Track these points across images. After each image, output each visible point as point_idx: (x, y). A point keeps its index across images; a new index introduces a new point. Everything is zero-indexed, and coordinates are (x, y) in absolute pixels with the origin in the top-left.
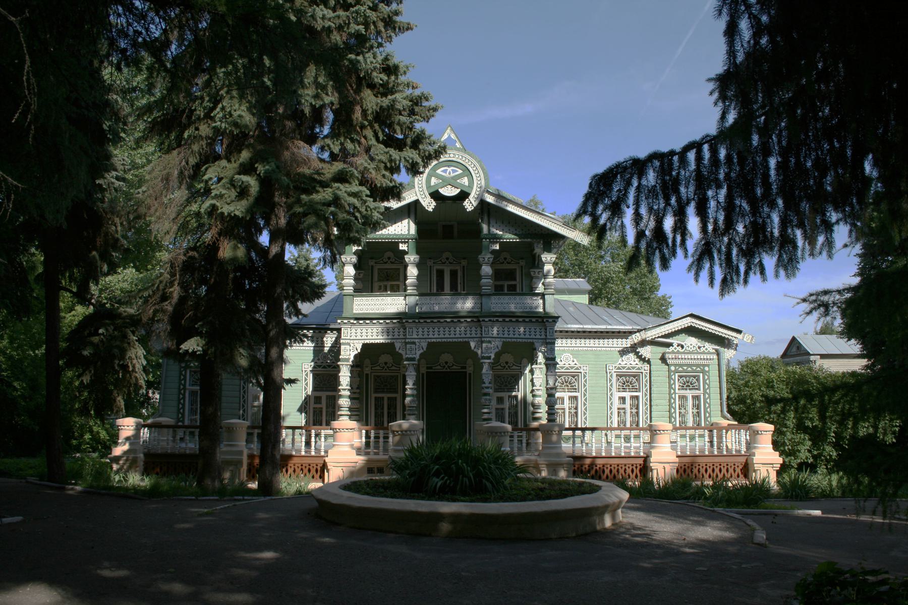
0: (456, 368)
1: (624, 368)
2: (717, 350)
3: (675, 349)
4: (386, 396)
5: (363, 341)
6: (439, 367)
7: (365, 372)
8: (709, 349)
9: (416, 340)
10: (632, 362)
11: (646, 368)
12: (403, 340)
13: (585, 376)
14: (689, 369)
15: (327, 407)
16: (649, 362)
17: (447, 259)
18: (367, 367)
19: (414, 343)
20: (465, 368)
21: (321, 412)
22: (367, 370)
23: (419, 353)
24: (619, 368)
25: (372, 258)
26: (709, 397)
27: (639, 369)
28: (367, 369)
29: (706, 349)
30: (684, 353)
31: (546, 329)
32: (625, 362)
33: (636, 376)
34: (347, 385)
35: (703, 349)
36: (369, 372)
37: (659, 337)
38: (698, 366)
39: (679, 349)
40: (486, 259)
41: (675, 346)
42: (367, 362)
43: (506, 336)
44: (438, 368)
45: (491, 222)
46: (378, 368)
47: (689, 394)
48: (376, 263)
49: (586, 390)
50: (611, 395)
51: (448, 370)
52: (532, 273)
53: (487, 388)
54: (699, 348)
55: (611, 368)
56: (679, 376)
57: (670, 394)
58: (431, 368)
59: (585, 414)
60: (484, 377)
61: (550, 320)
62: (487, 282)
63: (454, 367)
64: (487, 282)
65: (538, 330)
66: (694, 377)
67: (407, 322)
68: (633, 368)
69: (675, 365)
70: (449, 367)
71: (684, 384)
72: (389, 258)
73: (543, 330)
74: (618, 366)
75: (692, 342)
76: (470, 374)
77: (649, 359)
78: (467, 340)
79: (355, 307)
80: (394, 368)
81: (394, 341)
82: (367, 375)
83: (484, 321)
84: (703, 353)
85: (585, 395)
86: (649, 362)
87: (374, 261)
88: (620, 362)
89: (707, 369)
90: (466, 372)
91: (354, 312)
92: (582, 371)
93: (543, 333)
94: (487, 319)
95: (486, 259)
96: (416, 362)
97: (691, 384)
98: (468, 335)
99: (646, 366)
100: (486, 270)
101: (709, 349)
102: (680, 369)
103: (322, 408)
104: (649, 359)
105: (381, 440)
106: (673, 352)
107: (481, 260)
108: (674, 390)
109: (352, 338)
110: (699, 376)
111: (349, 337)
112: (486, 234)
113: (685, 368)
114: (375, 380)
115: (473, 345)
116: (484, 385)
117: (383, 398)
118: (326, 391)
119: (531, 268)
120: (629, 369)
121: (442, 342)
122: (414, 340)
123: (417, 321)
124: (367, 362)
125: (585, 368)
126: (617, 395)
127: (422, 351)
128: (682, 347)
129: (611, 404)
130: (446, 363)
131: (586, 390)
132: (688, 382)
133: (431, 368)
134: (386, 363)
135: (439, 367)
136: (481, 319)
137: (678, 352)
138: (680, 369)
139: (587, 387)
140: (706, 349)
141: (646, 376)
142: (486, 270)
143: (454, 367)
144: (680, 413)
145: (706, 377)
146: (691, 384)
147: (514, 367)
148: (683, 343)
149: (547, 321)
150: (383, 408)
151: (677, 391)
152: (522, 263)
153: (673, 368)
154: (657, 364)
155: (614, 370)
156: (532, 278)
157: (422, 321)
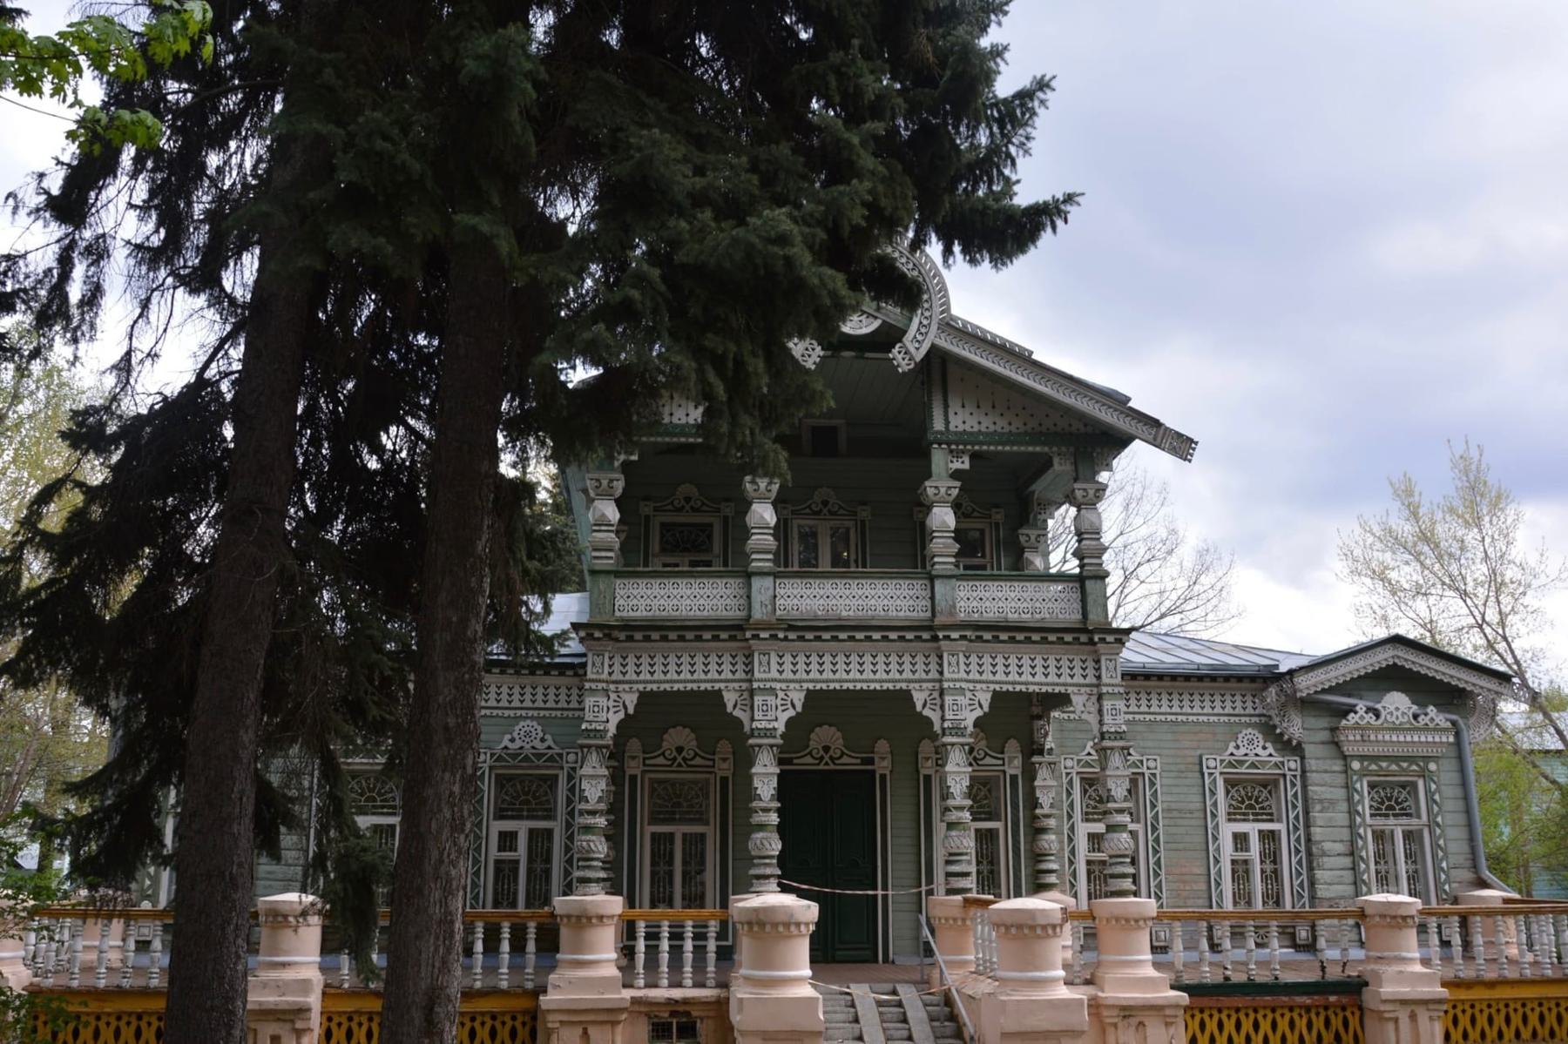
0: (850, 762)
1: (1241, 763)
2: (1454, 723)
3: (1362, 718)
4: (679, 830)
5: (641, 687)
6: (808, 760)
7: (629, 772)
8: (1437, 721)
9: (778, 686)
10: (1259, 751)
11: (1293, 765)
12: (744, 685)
13: (1152, 784)
14: (1394, 767)
15: (530, 860)
16: (1296, 749)
17: (825, 503)
18: (634, 758)
19: (772, 691)
20: (871, 761)
21: (515, 871)
22: (633, 768)
23: (784, 717)
24: (1230, 765)
25: (646, 498)
26: (1443, 835)
28: (633, 763)
29: (1432, 720)
30: (1378, 729)
31: (1098, 661)
32: (1243, 751)
33: (1270, 784)
34: (600, 799)
35: (1423, 720)
36: (638, 772)
37: (1324, 691)
38: (1411, 759)
39: (1370, 718)
40: (943, 490)
41: (1361, 712)
42: (634, 745)
43: (1000, 677)
44: (805, 762)
45: (950, 403)
46: (661, 760)
47: (1397, 827)
48: (656, 509)
49: (1156, 817)
50: (1216, 827)
51: (832, 767)
52: (1022, 539)
53: (961, 808)
54: (1415, 717)
55: (1212, 763)
57: (1352, 826)
58: (789, 761)
59: (1157, 875)
60: (950, 782)
61: (1110, 638)
62: (943, 549)
63: (845, 760)
64: (943, 549)
65: (1077, 664)
66: (1403, 786)
67: (756, 637)
68: (1264, 763)
69: (1362, 758)
70: (831, 758)
71: (1382, 803)
72: (688, 500)
73: (1090, 664)
74: (1228, 758)
75: (1397, 703)
76: (883, 777)
77: (1299, 744)
78: (904, 686)
79: (619, 602)
80: (698, 761)
81: (722, 686)
82: (633, 778)
83: (947, 638)
84: (1426, 729)
85: (1154, 829)
86: (1296, 749)
87: (652, 505)
88: (1231, 749)
89: (1432, 766)
90: (873, 772)
91: (617, 614)
92: (1144, 770)
93: (1090, 672)
94: (955, 635)
95: (943, 490)
96: (780, 741)
98: (907, 675)
99: (1293, 764)
100: (943, 518)
101: (1437, 721)
102: (1373, 767)
103: (517, 862)
104: (1299, 744)
105: (665, 945)
106: (1357, 727)
107: (930, 491)
108: (1363, 816)
109: (614, 677)
110: (1414, 785)
111: (605, 676)
112: (941, 433)
113: (1384, 765)
114: (653, 791)
115: (919, 698)
116: (950, 802)
117: (672, 835)
118: (528, 818)
119: (1021, 526)
120: (1253, 765)
121: (841, 691)
122: (774, 685)
123: (781, 635)
124: (634, 745)
125: (1152, 764)
126: (1227, 830)
127: (791, 713)
128: (1378, 716)
129: (1218, 849)
130: (826, 749)
131: (1156, 817)
132: (1389, 799)
133: (789, 761)
134: (680, 750)
135: (808, 760)
136: (941, 635)
137: (1369, 727)
138: (1373, 767)
139: (1159, 808)
141: (1293, 785)
142: (943, 518)
143: (845, 760)
144: (1377, 872)
145: (1433, 787)
146: (1398, 803)
147: (988, 760)
148: (1378, 706)
149: (1103, 640)
150: (671, 862)
151: (1368, 820)
152: (998, 516)
153: (1356, 765)
154: (1318, 758)
155: (1220, 769)
156: (1021, 551)
157: (792, 636)
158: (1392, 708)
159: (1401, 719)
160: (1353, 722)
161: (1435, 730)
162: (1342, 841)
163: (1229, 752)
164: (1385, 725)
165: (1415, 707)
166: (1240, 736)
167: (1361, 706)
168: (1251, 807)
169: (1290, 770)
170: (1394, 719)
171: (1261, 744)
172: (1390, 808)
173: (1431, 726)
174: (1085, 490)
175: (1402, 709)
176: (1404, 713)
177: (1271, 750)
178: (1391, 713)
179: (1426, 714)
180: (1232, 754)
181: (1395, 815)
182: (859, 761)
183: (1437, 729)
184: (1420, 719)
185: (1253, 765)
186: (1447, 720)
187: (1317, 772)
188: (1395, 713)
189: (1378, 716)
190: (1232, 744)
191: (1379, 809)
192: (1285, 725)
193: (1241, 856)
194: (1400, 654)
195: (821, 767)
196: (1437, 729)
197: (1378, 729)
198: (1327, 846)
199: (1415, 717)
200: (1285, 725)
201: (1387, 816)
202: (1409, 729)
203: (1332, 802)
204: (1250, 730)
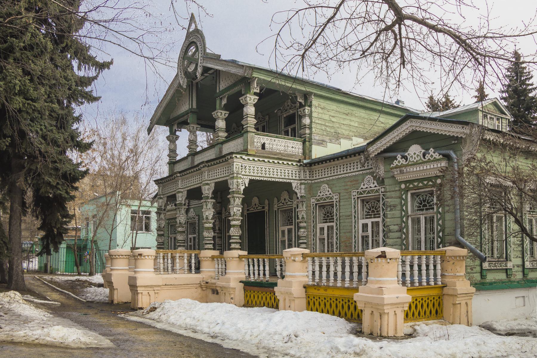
1: (364, 192)
14: (421, 185)
27: (377, 191)
30: (406, 166)
35: (428, 157)
39: (403, 162)
51: (257, 211)
54: (424, 155)
56: (412, 194)
68: (372, 191)
69: (405, 182)
76: (267, 212)
84: (429, 161)
88: (362, 186)
90: (264, 211)
97: (424, 201)
102: (411, 186)
106: (397, 167)
120: (369, 192)
128: (406, 160)
132: (424, 201)
137: (402, 166)
140: (432, 156)
148: (406, 154)
153: (403, 186)
158: (412, 154)
159: (417, 159)
160: (395, 164)
161: (433, 161)
162: (397, 225)
163: (361, 188)
164: (410, 163)
165: (423, 151)
166: (365, 179)
167: (399, 156)
168: (373, 211)
169: (382, 192)
170: (413, 159)
171: (372, 182)
172: (425, 206)
173: (432, 159)
174: (221, 113)
175: (417, 153)
176: (418, 155)
177: (376, 184)
178: (412, 157)
179: (429, 154)
180: (362, 188)
181: (427, 209)
182: (261, 208)
183: (436, 160)
184: (426, 157)
185: (369, 192)
186: (440, 154)
187: (390, 192)
188: (414, 156)
189: (406, 160)
190: (363, 184)
191: (420, 207)
192: (377, 171)
193: (365, 234)
194: (414, 124)
195: (255, 211)
196: (436, 160)
197: (406, 166)
198: (392, 227)
199: (424, 155)
200: (377, 171)
201: (422, 210)
202: (420, 163)
203: (395, 206)
204: (369, 176)
